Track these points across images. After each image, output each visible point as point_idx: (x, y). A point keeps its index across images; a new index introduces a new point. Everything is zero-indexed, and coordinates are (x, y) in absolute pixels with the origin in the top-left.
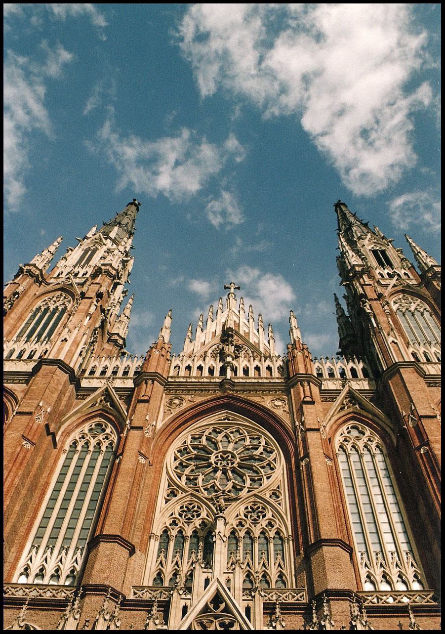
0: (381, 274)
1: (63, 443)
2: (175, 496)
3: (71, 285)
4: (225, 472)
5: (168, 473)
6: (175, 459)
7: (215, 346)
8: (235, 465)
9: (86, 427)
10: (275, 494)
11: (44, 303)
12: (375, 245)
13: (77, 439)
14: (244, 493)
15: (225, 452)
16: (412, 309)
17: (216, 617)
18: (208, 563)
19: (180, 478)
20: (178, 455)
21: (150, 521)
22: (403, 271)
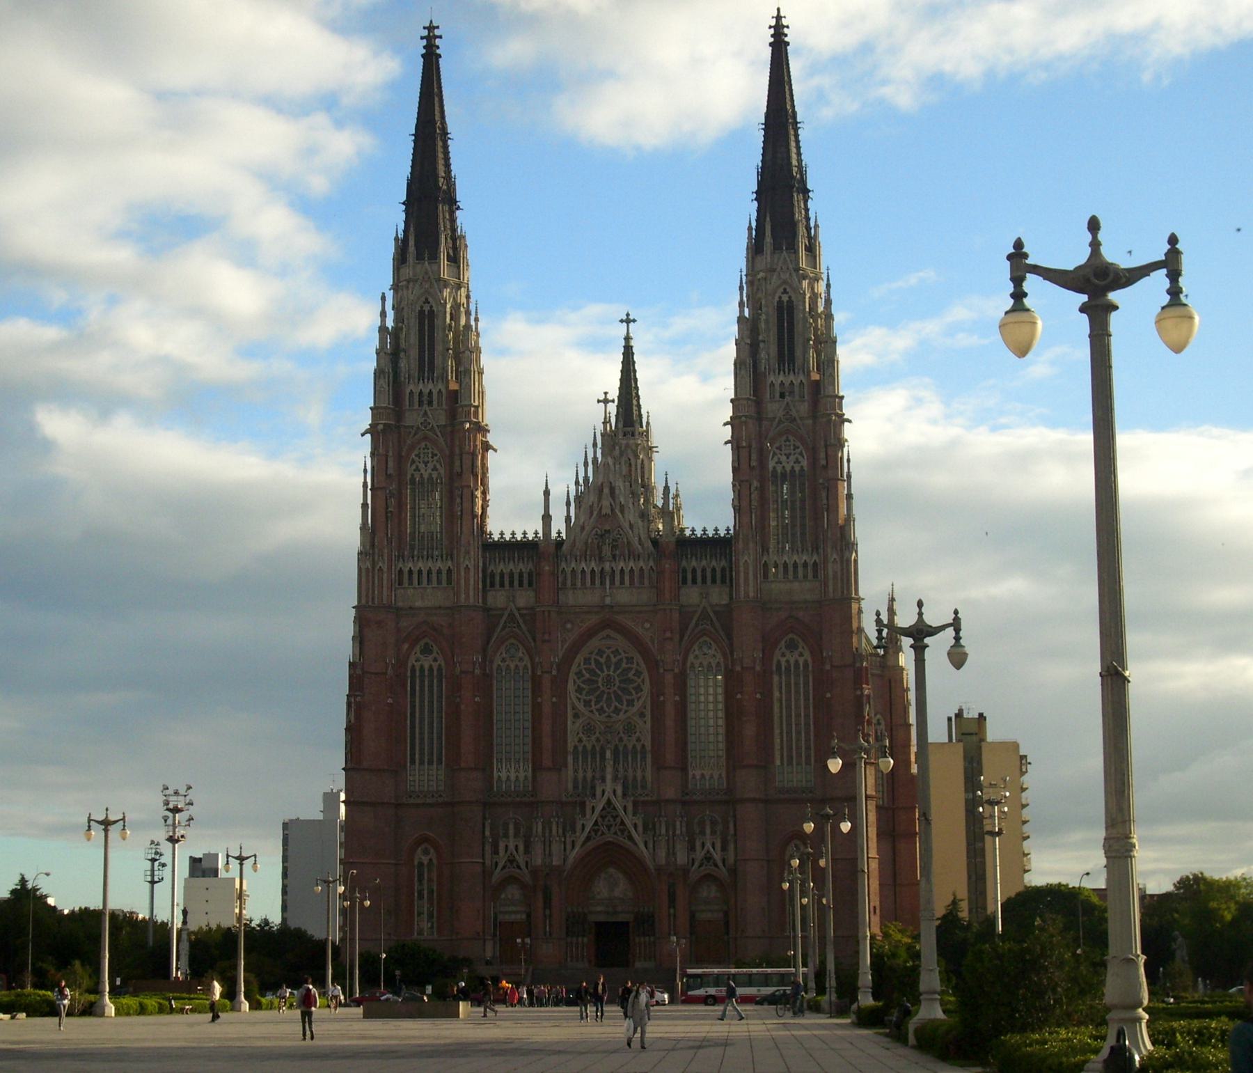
0: (772, 384)
1: (491, 669)
2: (578, 717)
3: (432, 429)
4: (609, 693)
5: (571, 699)
6: (575, 682)
7: (594, 532)
8: (616, 688)
9: (503, 649)
10: (642, 715)
11: (414, 467)
12: (785, 292)
13: (500, 663)
14: (621, 713)
15: (609, 675)
16: (788, 468)
17: (609, 813)
18: (603, 780)
19: (579, 699)
20: (575, 678)
21: (566, 742)
22: (802, 377)
